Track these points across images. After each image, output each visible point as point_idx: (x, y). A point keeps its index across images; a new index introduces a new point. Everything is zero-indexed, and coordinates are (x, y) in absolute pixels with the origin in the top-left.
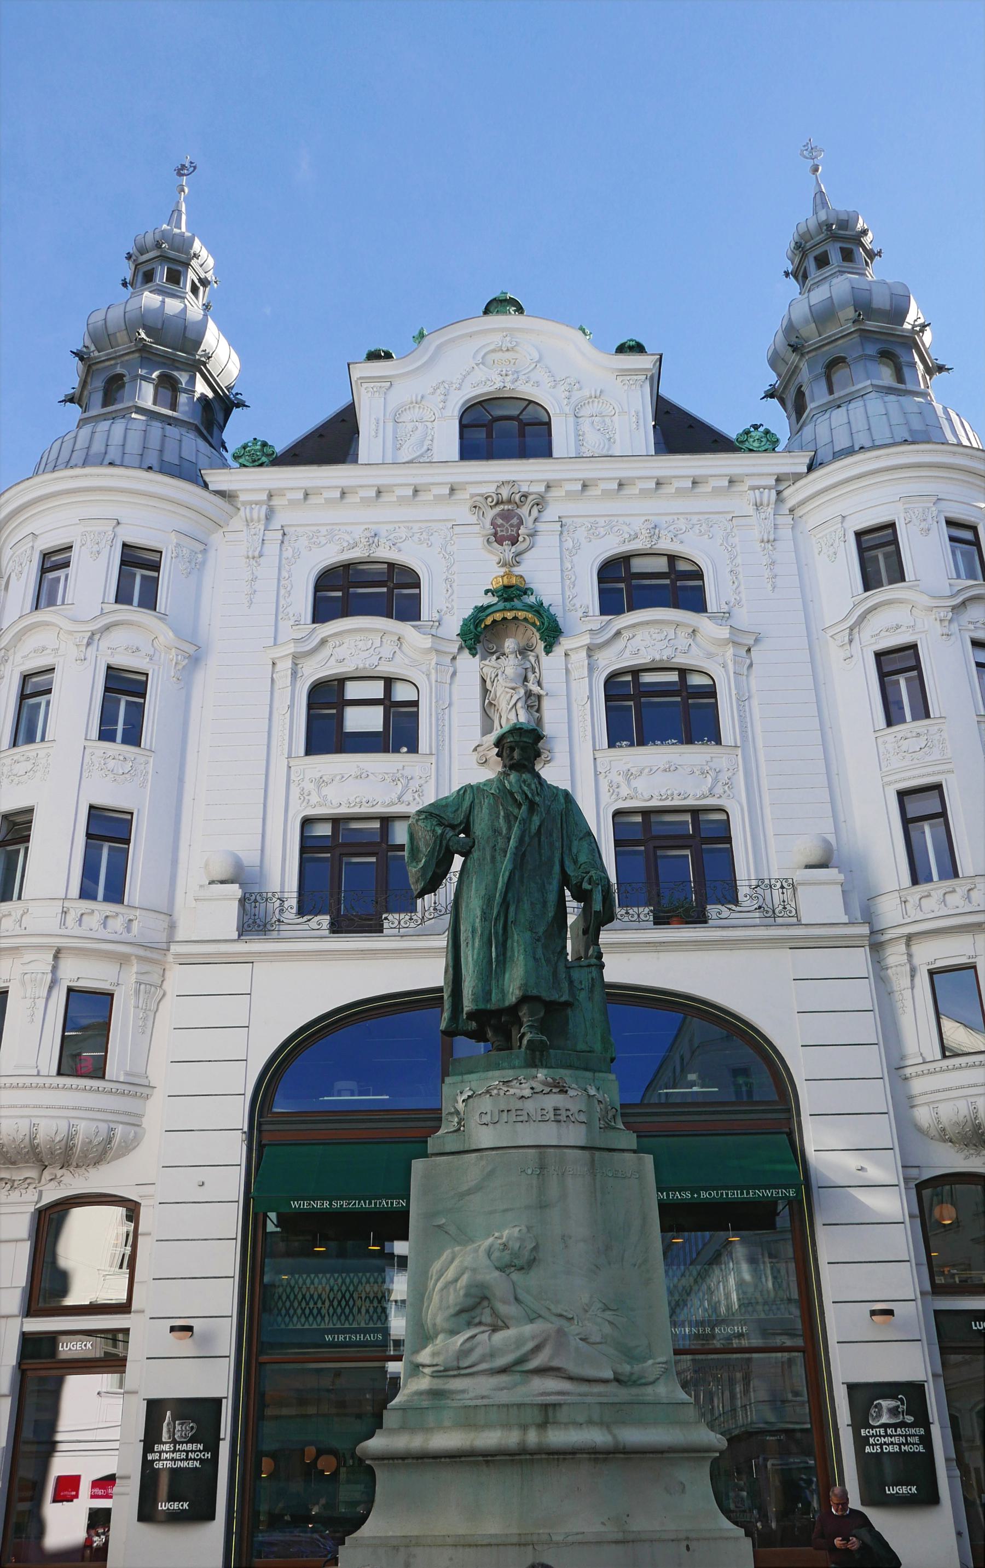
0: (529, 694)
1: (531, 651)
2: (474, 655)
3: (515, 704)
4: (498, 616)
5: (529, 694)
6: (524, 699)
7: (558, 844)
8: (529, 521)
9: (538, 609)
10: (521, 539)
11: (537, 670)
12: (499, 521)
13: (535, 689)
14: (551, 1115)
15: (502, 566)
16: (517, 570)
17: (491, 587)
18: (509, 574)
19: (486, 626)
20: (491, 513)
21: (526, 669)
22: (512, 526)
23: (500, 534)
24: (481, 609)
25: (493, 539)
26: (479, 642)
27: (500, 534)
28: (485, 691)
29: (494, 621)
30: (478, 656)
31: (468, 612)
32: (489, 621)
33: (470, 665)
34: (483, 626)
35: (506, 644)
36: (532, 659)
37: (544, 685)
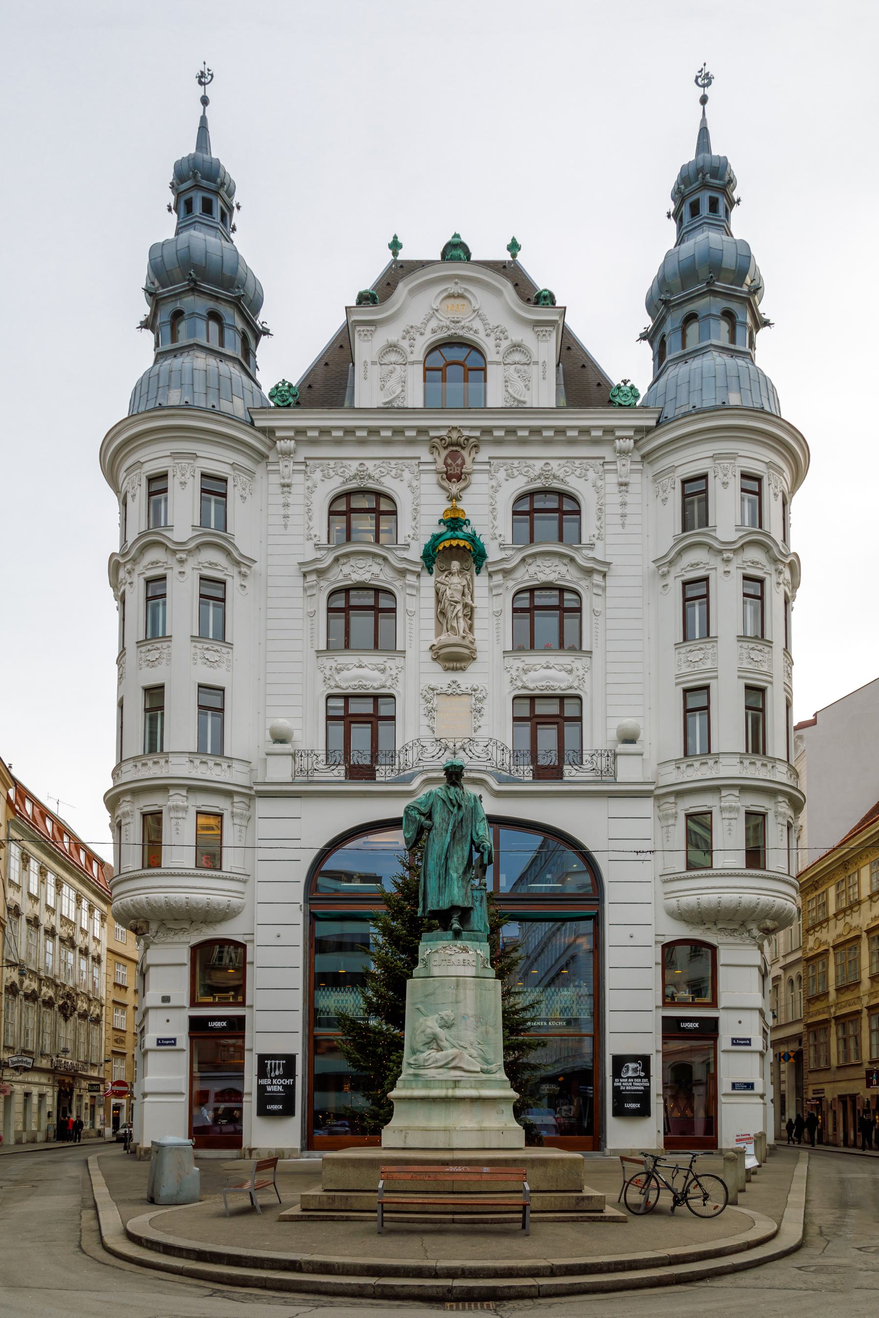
0: (465, 606)
1: (467, 570)
2: (431, 573)
3: (457, 614)
4: (447, 544)
5: (465, 606)
6: (462, 610)
7: (470, 826)
8: (468, 460)
9: (472, 539)
10: (463, 477)
11: (471, 587)
12: (449, 461)
13: (470, 602)
14: (462, 963)
15: (451, 500)
16: (460, 506)
17: (441, 518)
18: (454, 509)
19: (439, 551)
20: (444, 453)
21: (464, 586)
22: (457, 465)
23: (449, 472)
24: (436, 538)
25: (445, 476)
26: (435, 563)
27: (449, 472)
28: (438, 601)
29: (445, 547)
30: (434, 574)
31: (427, 539)
32: (441, 548)
33: (428, 582)
34: (437, 551)
35: (452, 566)
36: (468, 577)
37: (475, 600)
